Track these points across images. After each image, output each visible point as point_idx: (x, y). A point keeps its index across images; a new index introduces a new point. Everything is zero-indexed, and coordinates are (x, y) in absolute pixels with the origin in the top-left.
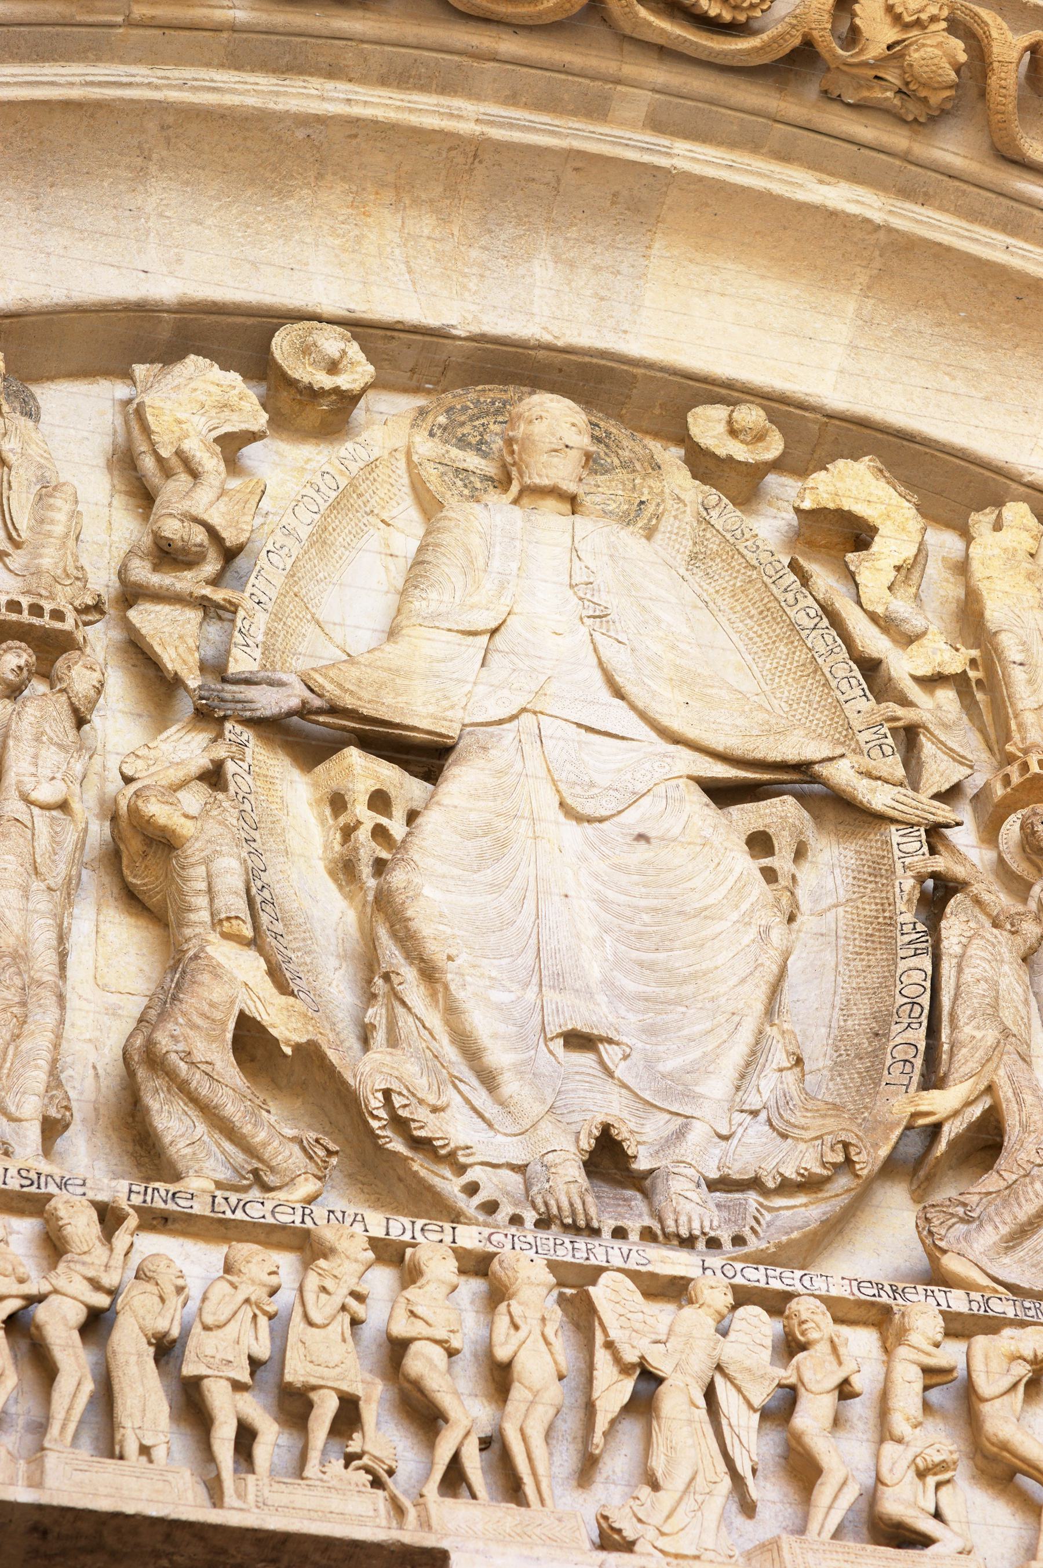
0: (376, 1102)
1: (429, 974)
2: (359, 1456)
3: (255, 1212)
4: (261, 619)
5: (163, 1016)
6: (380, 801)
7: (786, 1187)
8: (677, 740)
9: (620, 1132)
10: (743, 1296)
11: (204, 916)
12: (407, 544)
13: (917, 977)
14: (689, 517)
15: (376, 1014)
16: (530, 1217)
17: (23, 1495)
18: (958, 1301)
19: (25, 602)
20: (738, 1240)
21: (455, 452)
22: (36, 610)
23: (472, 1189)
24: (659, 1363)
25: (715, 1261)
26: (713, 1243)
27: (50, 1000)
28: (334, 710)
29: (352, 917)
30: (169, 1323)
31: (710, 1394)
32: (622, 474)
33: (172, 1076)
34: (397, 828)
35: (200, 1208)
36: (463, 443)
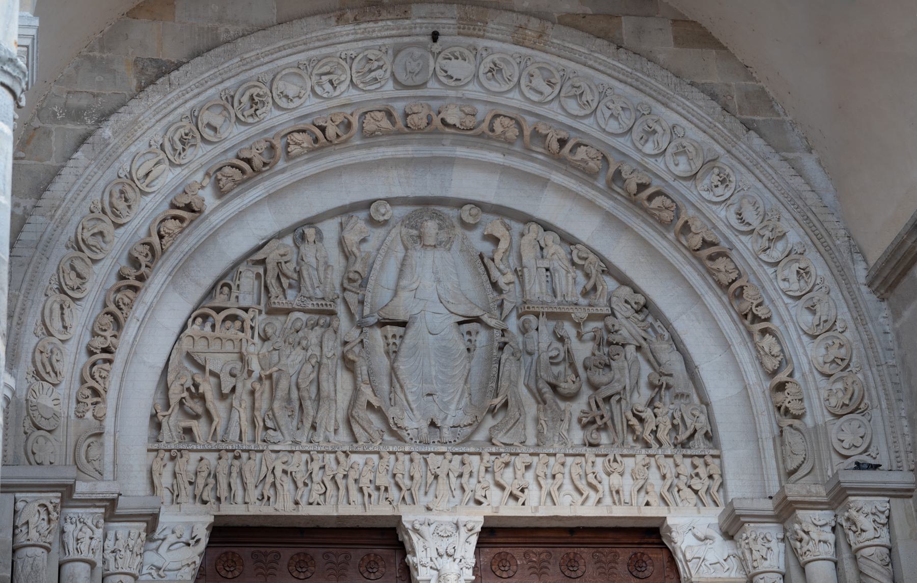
0: (391, 421)
1: (401, 387)
2: (387, 499)
3: (371, 449)
4: (370, 295)
5: (354, 407)
6: (394, 336)
7: (465, 426)
8: (452, 313)
9: (435, 420)
10: (454, 454)
11: (360, 379)
12: (401, 255)
13: (495, 369)
14: (460, 240)
15: (392, 395)
16: (418, 441)
17: (335, 514)
18: (494, 450)
19: (324, 303)
20: (455, 441)
21: (410, 230)
22: (326, 305)
23: (409, 434)
24: (438, 473)
25: (450, 448)
26: (450, 442)
27: (334, 402)
28: (384, 319)
29: (389, 363)
30: (357, 477)
31: (448, 474)
32: (446, 230)
33: (356, 419)
34: (398, 342)
35: (361, 449)
36: (412, 227)
